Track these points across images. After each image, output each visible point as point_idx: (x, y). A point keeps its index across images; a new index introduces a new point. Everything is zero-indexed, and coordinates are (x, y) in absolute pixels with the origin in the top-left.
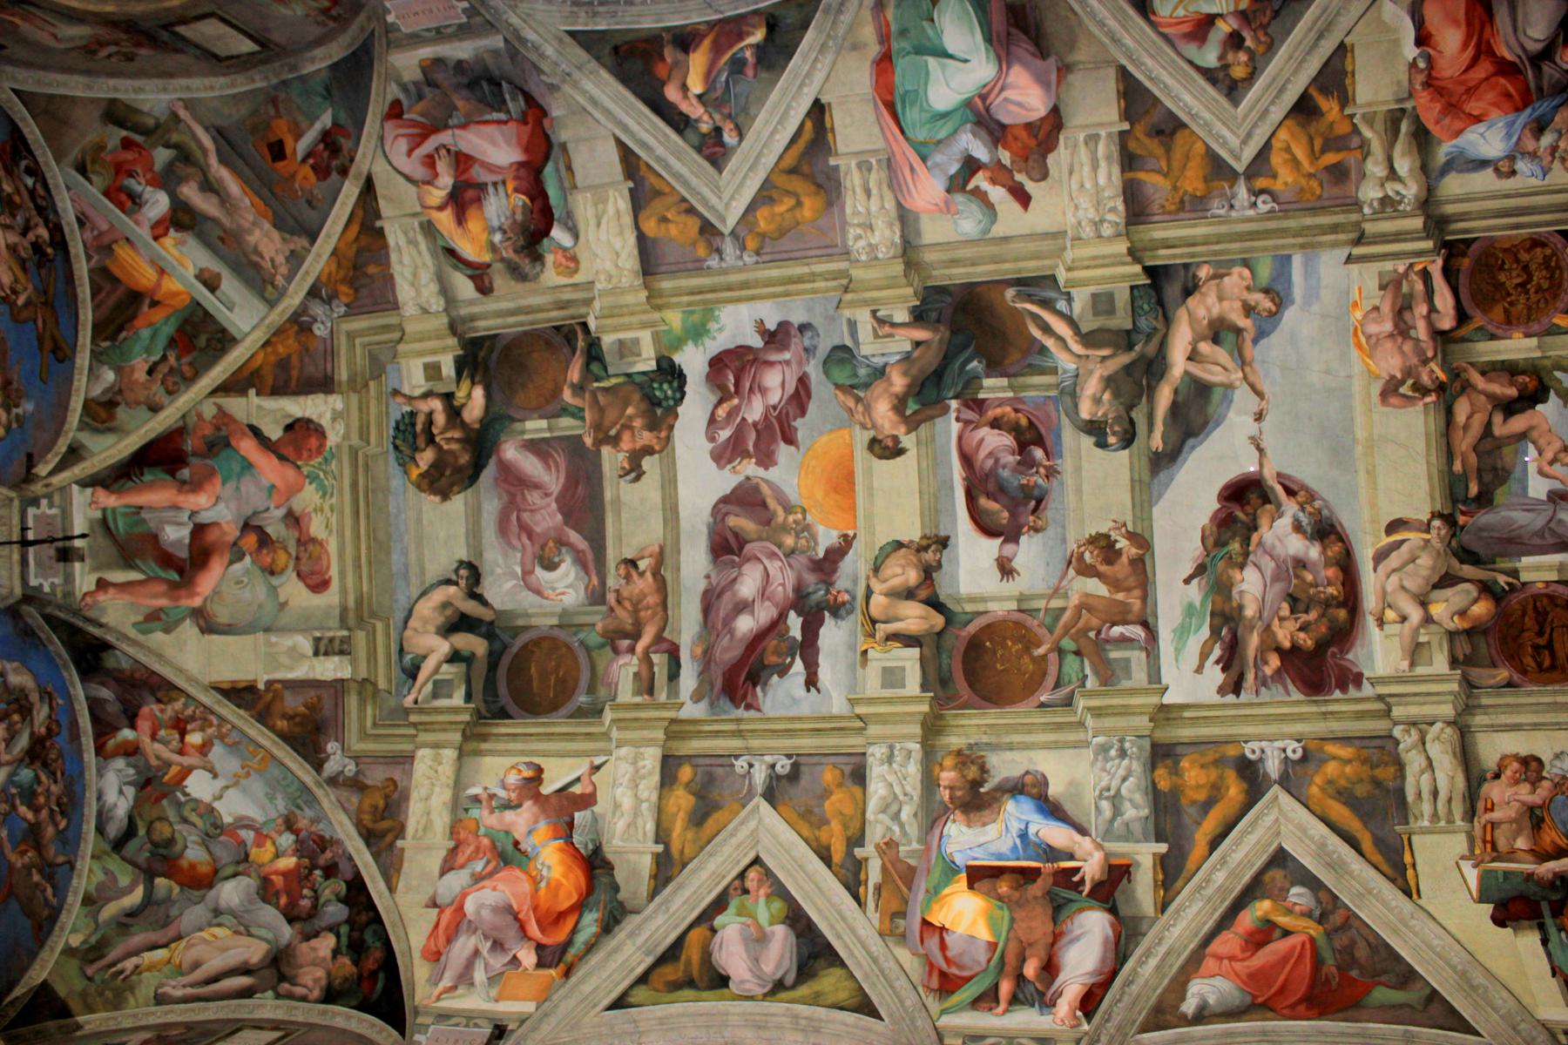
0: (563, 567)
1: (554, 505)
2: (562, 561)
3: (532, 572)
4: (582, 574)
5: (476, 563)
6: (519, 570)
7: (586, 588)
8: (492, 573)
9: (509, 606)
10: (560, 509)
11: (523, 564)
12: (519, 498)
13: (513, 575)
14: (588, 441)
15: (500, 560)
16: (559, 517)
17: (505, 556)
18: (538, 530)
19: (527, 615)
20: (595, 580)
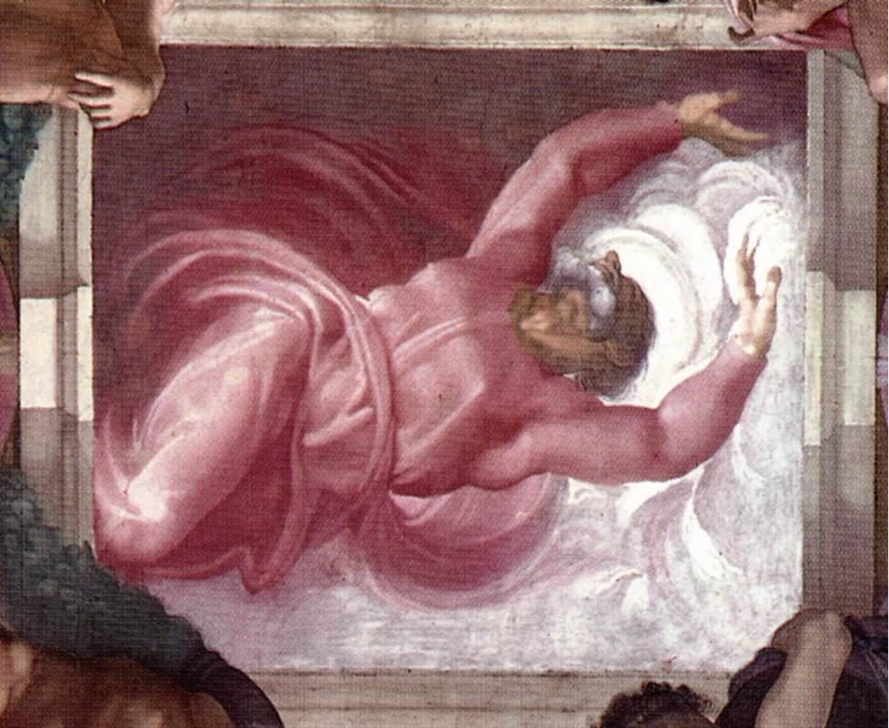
0: (639, 265)
1: (378, 301)
2: (613, 273)
3: (649, 416)
4: (670, 172)
5: (602, 701)
6: (640, 493)
7: (732, 150)
8: (641, 628)
9: (790, 546)
10: (398, 270)
11: (613, 473)
12: (342, 480)
13: (658, 521)
14: (126, 101)
15: (589, 585)
16: (429, 278)
17: (581, 560)
18: (475, 388)
19: (834, 437)
20: (698, 106)
